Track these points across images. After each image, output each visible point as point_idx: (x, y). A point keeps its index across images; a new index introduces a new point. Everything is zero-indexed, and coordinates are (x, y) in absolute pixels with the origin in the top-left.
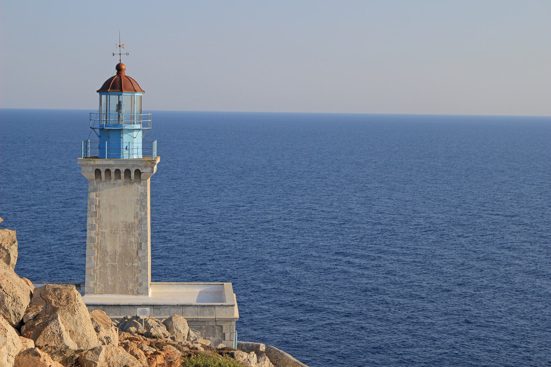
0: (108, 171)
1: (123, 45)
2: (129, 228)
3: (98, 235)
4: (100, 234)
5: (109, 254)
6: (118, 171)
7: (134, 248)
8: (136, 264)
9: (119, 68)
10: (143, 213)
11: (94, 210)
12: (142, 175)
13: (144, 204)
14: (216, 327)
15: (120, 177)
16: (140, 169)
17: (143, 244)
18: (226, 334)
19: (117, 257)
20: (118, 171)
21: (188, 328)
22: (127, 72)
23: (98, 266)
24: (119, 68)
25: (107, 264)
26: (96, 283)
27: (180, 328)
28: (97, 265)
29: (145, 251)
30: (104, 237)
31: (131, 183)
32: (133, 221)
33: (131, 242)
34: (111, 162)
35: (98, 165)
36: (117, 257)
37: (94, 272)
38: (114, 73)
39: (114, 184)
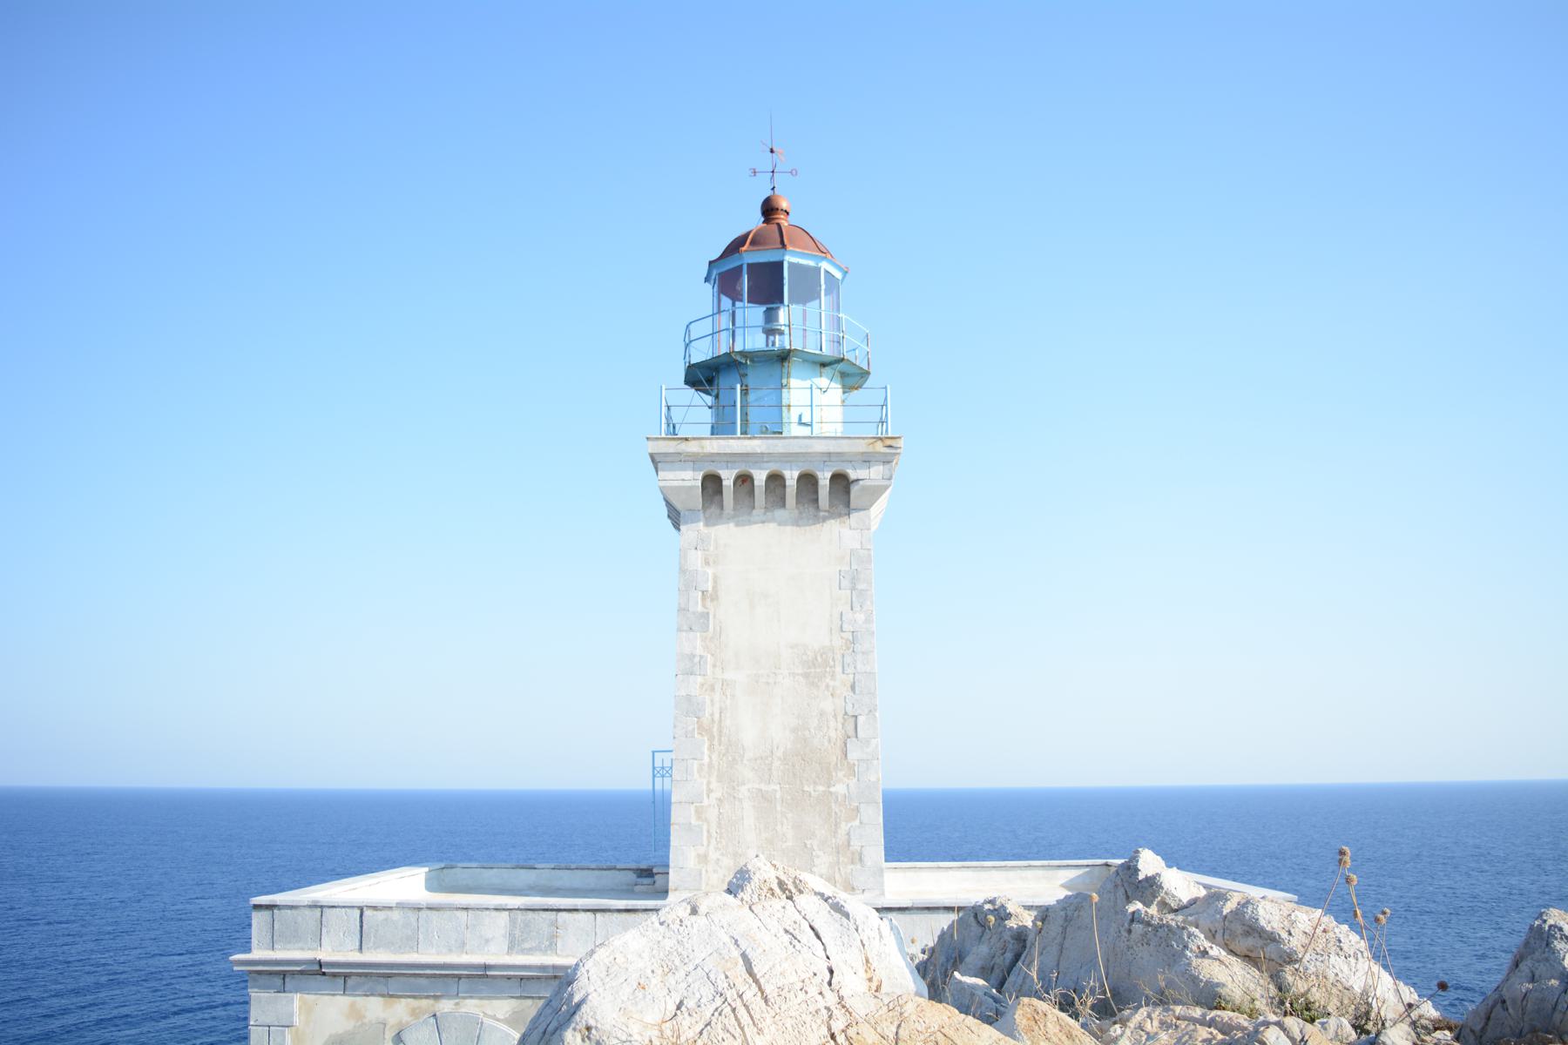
0: (744, 480)
2: (815, 668)
3: (713, 689)
4: (718, 687)
7: (833, 734)
8: (839, 789)
11: (700, 608)
12: (854, 489)
15: (782, 502)
17: (861, 720)
19: (777, 763)
22: (797, 212)
23: (713, 795)
25: (743, 789)
28: (710, 791)
30: (733, 696)
31: (817, 519)
33: (822, 714)
35: (712, 458)
36: (777, 763)
37: (699, 818)
38: (753, 221)
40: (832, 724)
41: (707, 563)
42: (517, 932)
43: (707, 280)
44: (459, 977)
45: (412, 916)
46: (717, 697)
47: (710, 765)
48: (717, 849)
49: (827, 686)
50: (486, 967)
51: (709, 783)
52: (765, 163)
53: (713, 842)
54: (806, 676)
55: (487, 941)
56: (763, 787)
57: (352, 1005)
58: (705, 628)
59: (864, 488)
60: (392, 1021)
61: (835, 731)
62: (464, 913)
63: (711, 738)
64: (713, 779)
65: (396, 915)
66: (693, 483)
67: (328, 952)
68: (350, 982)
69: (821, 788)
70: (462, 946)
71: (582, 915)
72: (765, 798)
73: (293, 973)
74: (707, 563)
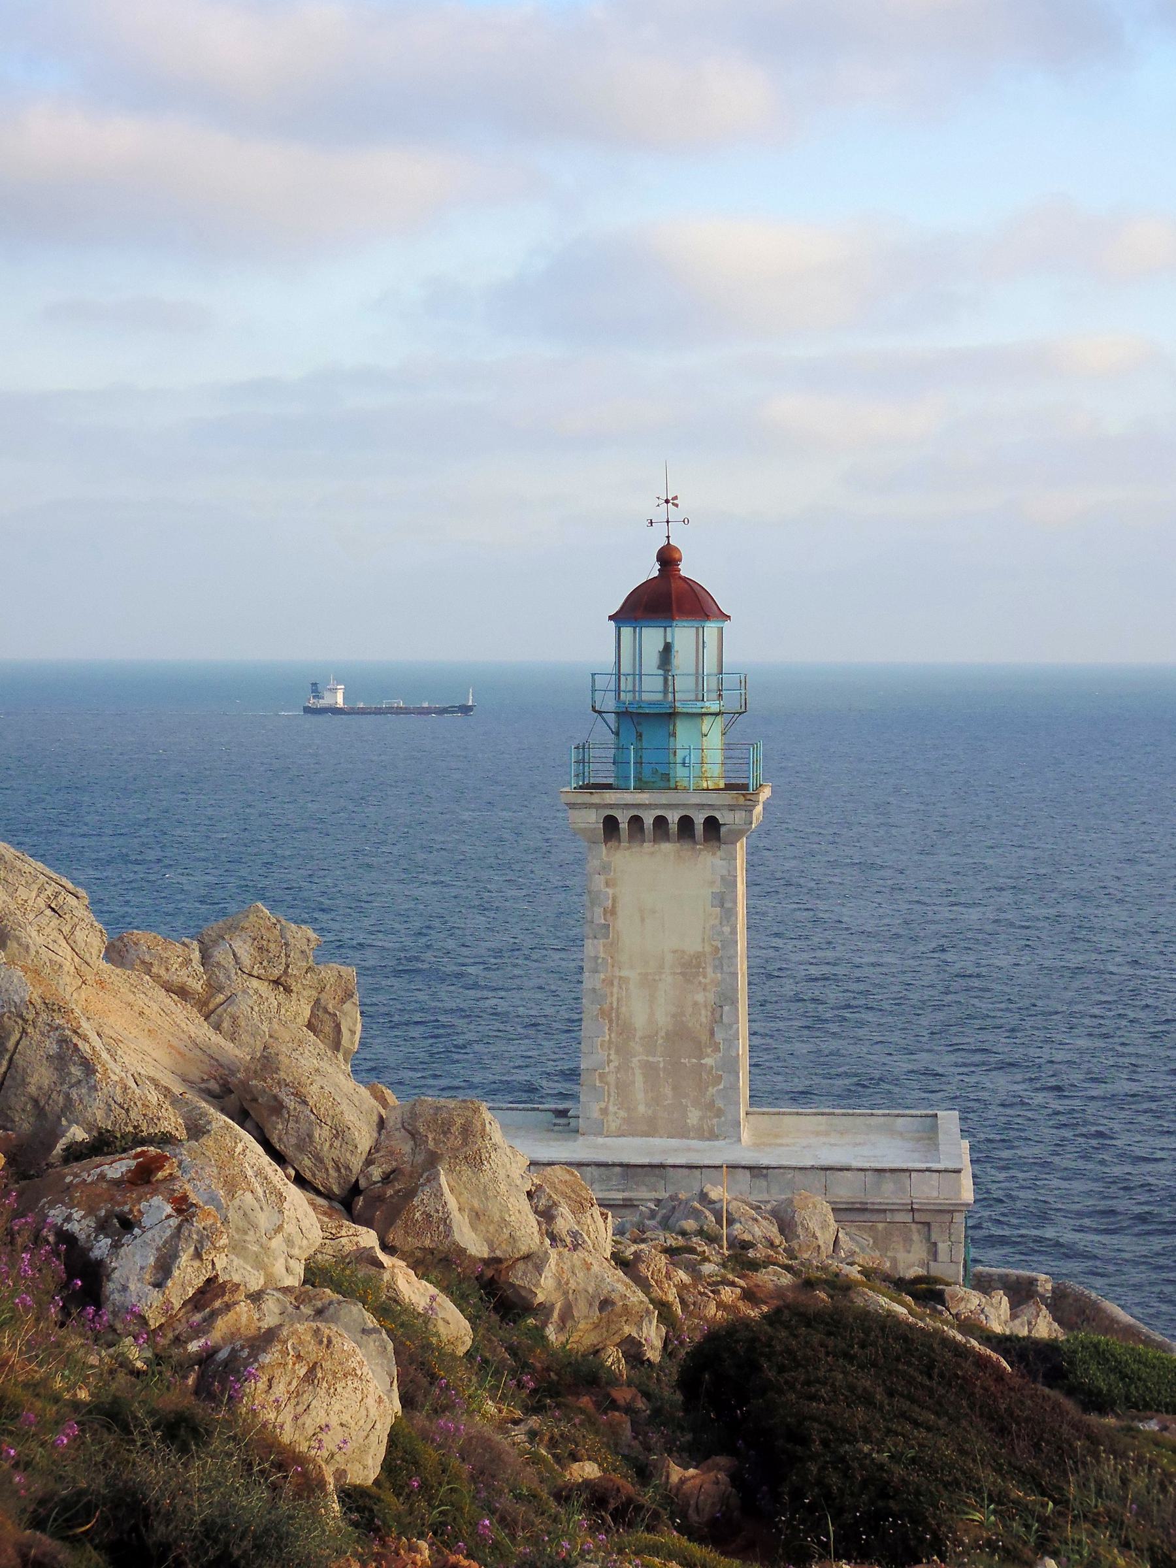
0: (636, 821)
1: (675, 498)
2: (690, 968)
3: (612, 984)
4: (616, 983)
5: (639, 1034)
7: (704, 1020)
8: (708, 1061)
9: (668, 558)
10: (727, 929)
11: (603, 921)
12: (723, 830)
14: (914, 1226)
16: (718, 815)
17: (726, 1008)
18: (940, 1245)
19: (660, 1041)
21: (833, 1226)
24: (668, 558)
25: (635, 1060)
27: (814, 1225)
28: (610, 1061)
29: (730, 1026)
32: (701, 950)
33: (696, 1004)
34: (644, 797)
36: (660, 1041)
37: (601, 1081)
39: (652, 853)
40: (703, 1012)
41: (607, 885)
46: (615, 990)
47: (610, 1041)
48: (615, 1105)
49: (700, 983)
51: (609, 1055)
52: (660, 513)
53: (612, 1099)
56: (651, 1059)
59: (730, 830)
61: (704, 1017)
63: (611, 1021)
64: (612, 1052)
66: (597, 825)
69: (694, 1060)
72: (650, 1069)
74: (607, 885)
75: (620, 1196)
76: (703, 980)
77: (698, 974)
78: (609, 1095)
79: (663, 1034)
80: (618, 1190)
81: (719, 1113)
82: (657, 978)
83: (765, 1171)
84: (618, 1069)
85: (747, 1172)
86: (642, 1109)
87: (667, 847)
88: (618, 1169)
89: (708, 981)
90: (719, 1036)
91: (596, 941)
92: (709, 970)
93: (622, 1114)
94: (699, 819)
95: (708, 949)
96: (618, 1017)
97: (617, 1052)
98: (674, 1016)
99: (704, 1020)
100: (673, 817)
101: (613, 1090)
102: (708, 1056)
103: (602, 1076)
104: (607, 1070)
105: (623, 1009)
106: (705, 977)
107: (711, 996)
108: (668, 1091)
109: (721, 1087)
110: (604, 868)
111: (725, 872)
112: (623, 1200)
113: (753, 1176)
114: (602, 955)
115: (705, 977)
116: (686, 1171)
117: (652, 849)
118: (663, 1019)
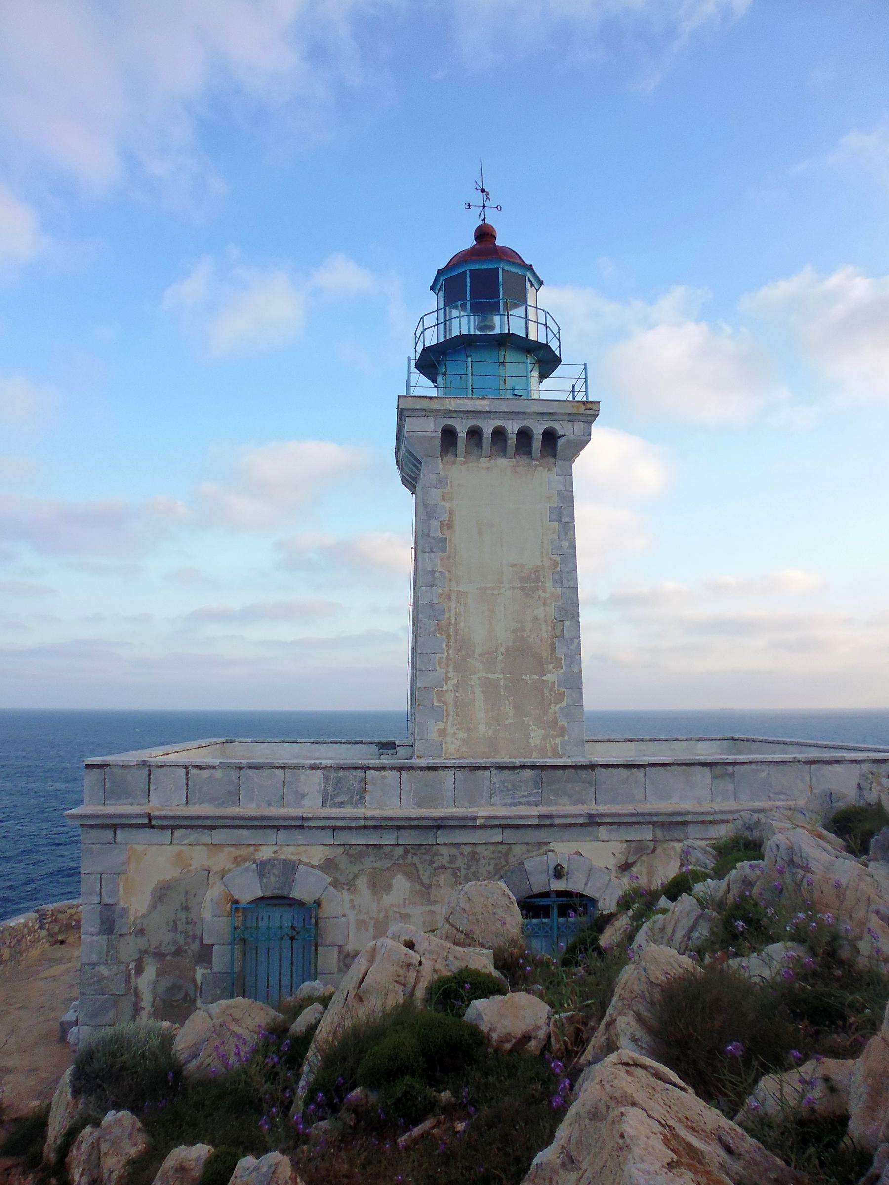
2: (529, 582)
3: (450, 598)
4: (453, 597)
6: (499, 434)
7: (545, 635)
8: (550, 678)
9: (484, 234)
10: (565, 544)
11: (440, 535)
12: (561, 442)
13: (565, 519)
16: (556, 426)
17: (567, 623)
19: (500, 657)
20: (499, 434)
23: (451, 683)
24: (484, 234)
25: (475, 677)
26: (445, 729)
28: (449, 679)
29: (572, 642)
30: (465, 605)
32: (540, 564)
33: (536, 619)
35: (450, 413)
36: (500, 657)
37: (439, 701)
39: (488, 468)
40: (544, 626)
42: (330, 788)
43: (432, 288)
44: (278, 828)
45: (233, 774)
46: (453, 604)
47: (448, 658)
49: (539, 597)
50: (304, 819)
51: (447, 672)
52: (477, 199)
54: (523, 589)
55: (303, 796)
56: (491, 676)
57: (179, 854)
58: (444, 550)
60: (216, 868)
61: (545, 632)
62: (279, 772)
63: (449, 637)
64: (451, 669)
65: (218, 774)
66: (434, 434)
67: (157, 805)
68: (178, 833)
69: (536, 677)
70: (282, 801)
71: (388, 773)
72: (490, 687)
73: (123, 826)
74: (444, 499)
75: (535, 811)
76: (543, 595)
77: (537, 588)
78: (448, 716)
79: (503, 650)
80: (529, 804)
81: (562, 732)
82: (496, 592)
83: (730, 769)
84: (457, 686)
85: (706, 770)
86: (482, 729)
87: (502, 462)
88: (529, 773)
89: (547, 595)
90: (560, 652)
91: (432, 555)
92: (549, 584)
93: (462, 735)
94: (538, 429)
95: (547, 564)
96: (456, 633)
97: (457, 669)
98: (514, 631)
99: (545, 635)
100: (512, 428)
101: (451, 708)
102: (549, 672)
103: (440, 694)
104: (445, 688)
105: (462, 625)
106: (544, 591)
107: (552, 611)
108: (509, 710)
109: (564, 704)
110: (440, 482)
111: (561, 488)
112: (541, 817)
113: (714, 777)
114: (439, 569)
115: (544, 591)
116: (624, 772)
117: (488, 465)
118: (503, 635)
